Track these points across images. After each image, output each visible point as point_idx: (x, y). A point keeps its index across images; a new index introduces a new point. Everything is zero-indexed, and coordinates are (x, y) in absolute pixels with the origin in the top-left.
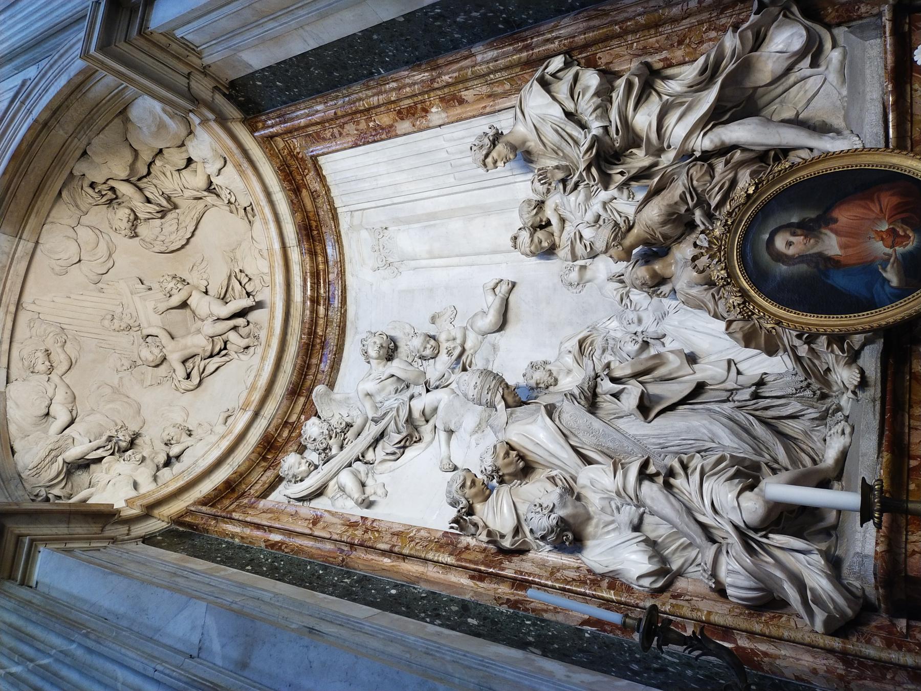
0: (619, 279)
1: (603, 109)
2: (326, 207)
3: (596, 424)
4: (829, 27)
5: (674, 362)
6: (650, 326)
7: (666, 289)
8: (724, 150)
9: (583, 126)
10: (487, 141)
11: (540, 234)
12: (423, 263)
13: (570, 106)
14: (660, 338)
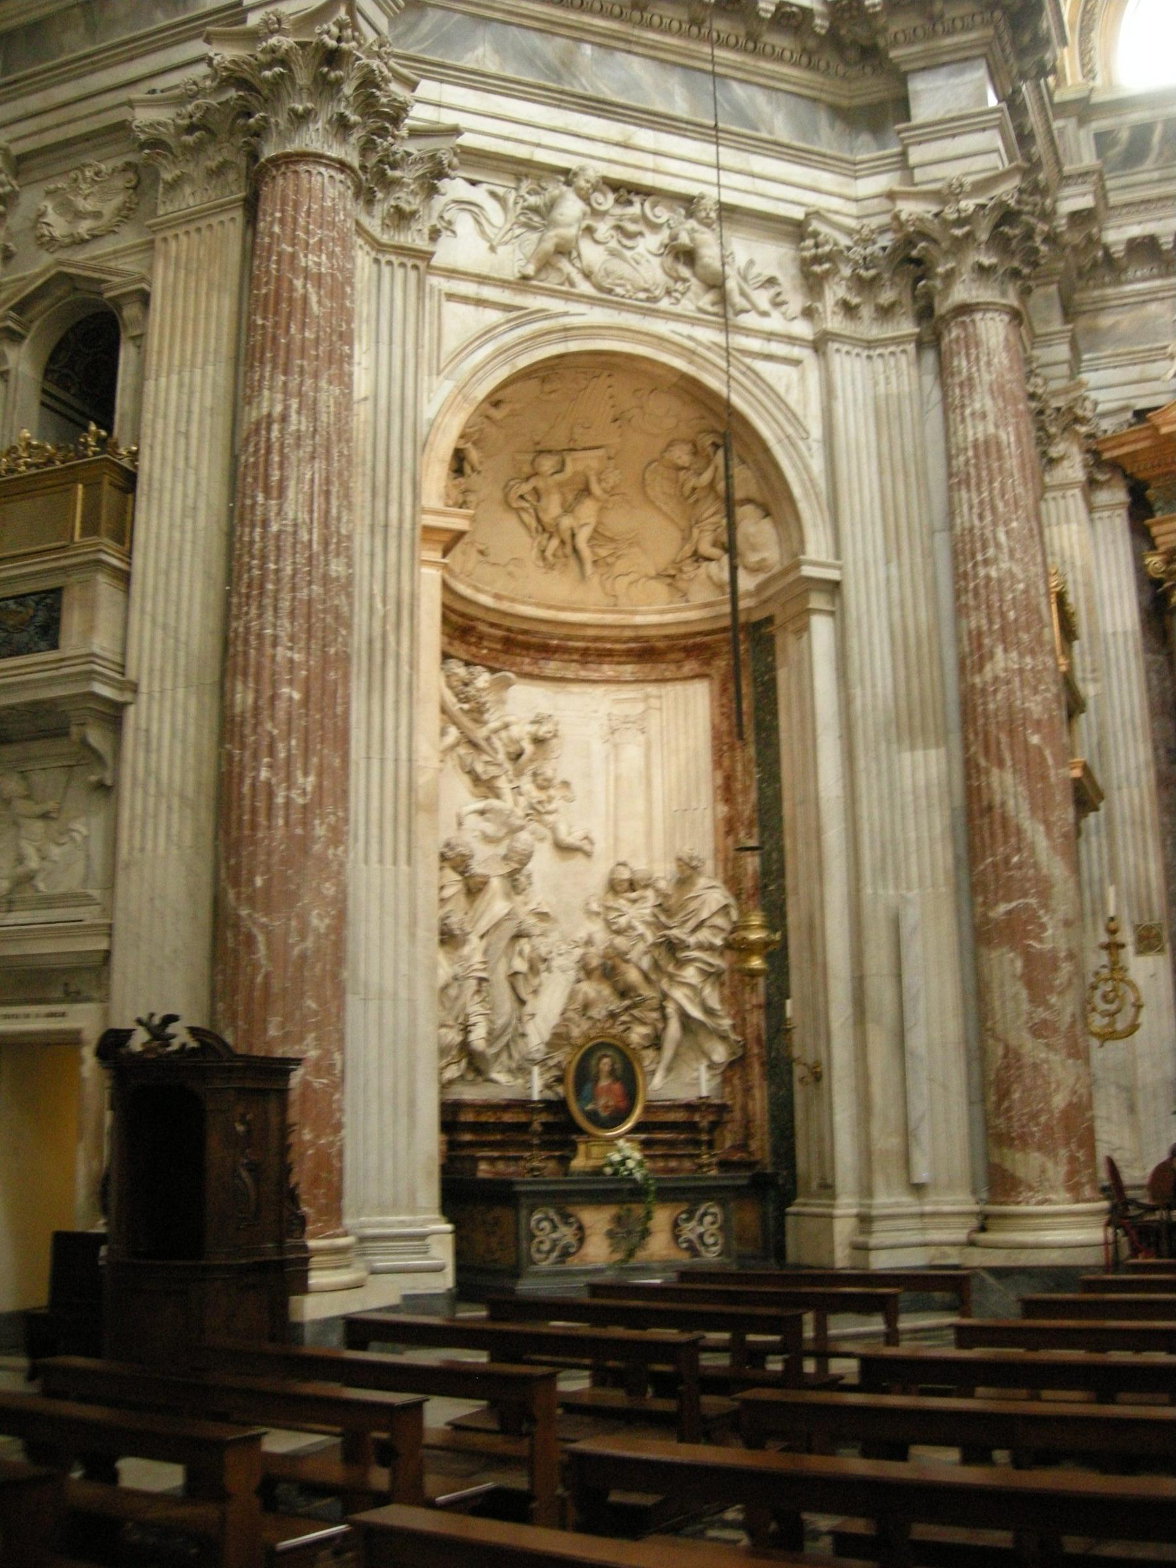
0: (589, 942)
1: (701, 947)
2: (668, 674)
3: (503, 943)
4: (723, 1073)
5: (535, 982)
6: (557, 962)
7: (582, 975)
8: (665, 1018)
9: (694, 930)
10: (694, 863)
11: (626, 885)
12: (612, 767)
13: (708, 923)
14: (549, 970)
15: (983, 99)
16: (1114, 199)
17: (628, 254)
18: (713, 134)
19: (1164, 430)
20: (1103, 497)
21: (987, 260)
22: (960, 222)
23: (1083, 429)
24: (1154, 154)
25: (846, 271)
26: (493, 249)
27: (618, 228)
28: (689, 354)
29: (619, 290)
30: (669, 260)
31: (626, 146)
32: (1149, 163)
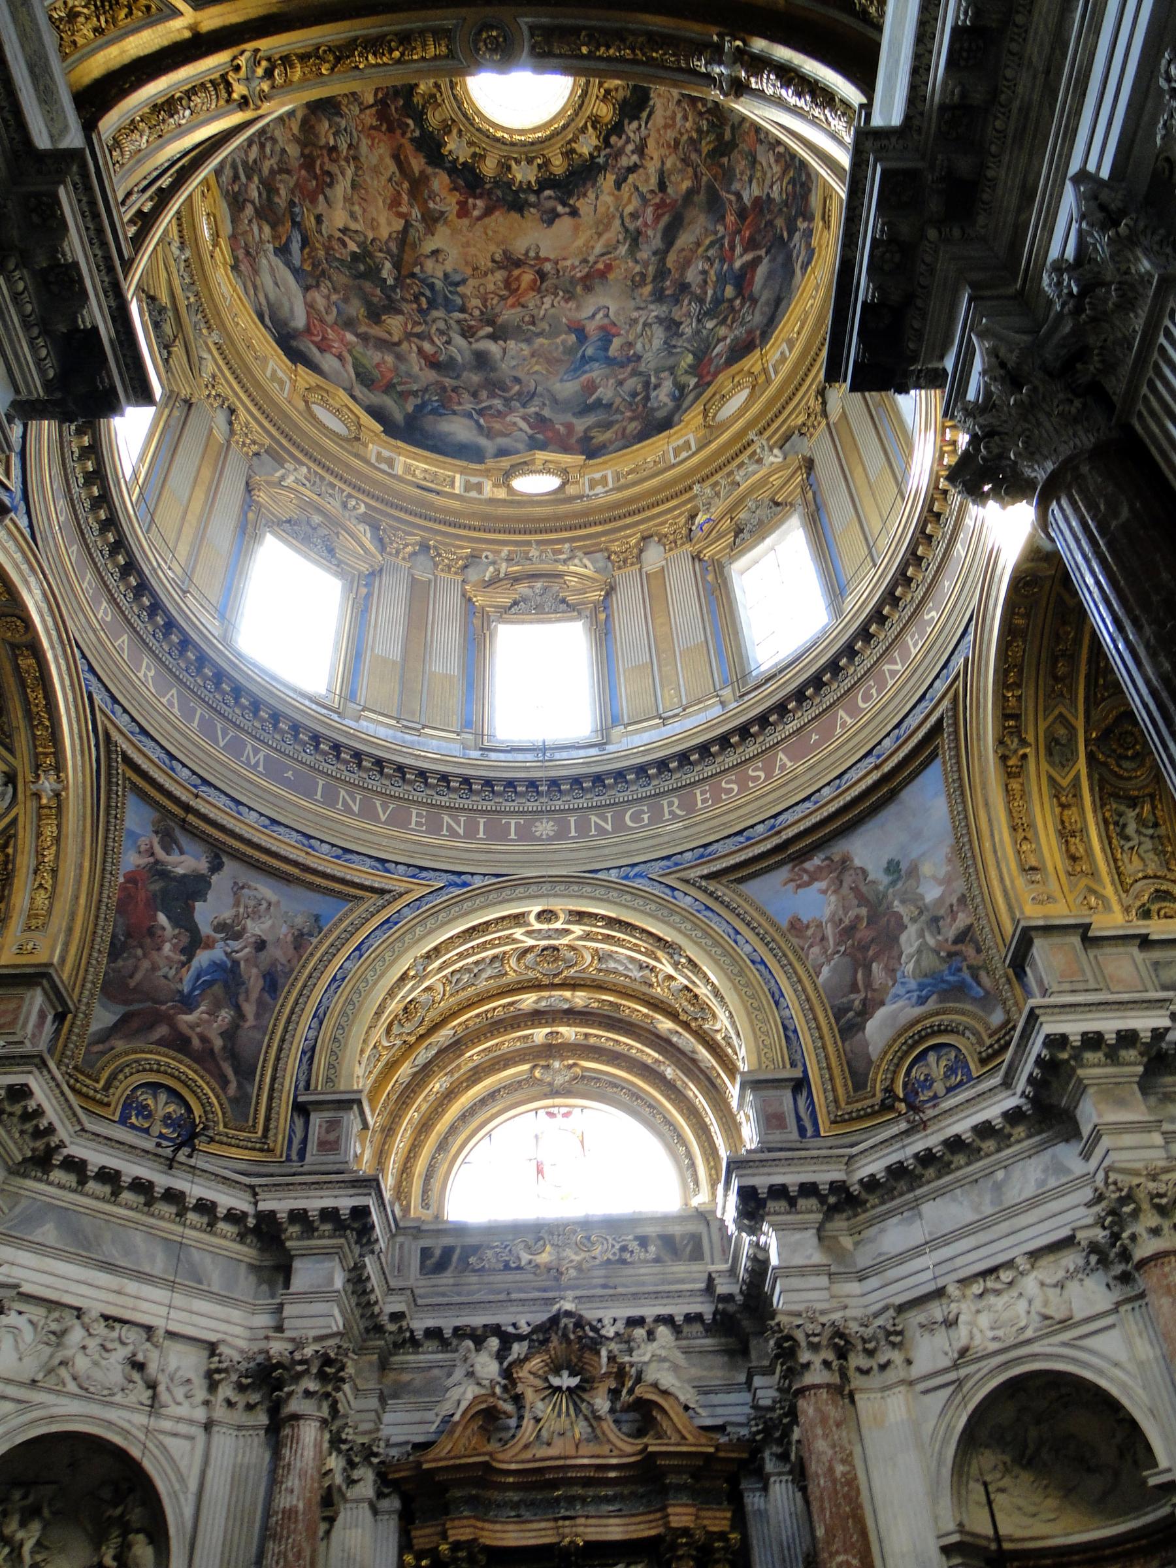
15: (331, 1281)
16: (420, 1301)
17: (104, 1363)
18: (172, 1286)
19: (425, 1466)
20: (385, 1504)
21: (313, 1386)
22: (301, 1362)
23: (375, 1460)
24: (451, 1268)
25: (234, 1377)
26: (20, 1359)
27: (102, 1345)
28: (125, 1433)
29: (92, 1389)
30: (128, 1368)
31: (119, 1293)
32: (448, 1273)
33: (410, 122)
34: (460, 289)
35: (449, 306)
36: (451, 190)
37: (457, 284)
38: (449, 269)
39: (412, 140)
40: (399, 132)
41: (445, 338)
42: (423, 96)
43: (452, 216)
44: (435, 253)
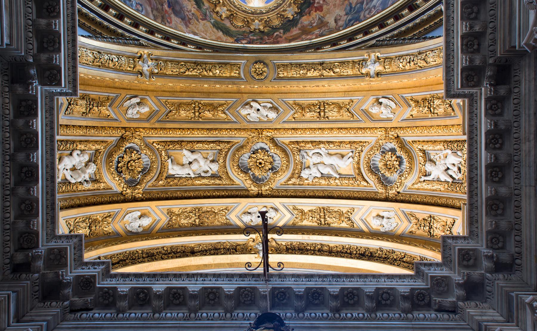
33: (275, 34)
34: (353, 6)
35: (359, 12)
36: (310, 15)
37: (351, 8)
38: (344, 13)
39: (284, 33)
40: (279, 39)
41: (373, 9)
42: (265, 27)
43: (321, 14)
44: (336, 21)
